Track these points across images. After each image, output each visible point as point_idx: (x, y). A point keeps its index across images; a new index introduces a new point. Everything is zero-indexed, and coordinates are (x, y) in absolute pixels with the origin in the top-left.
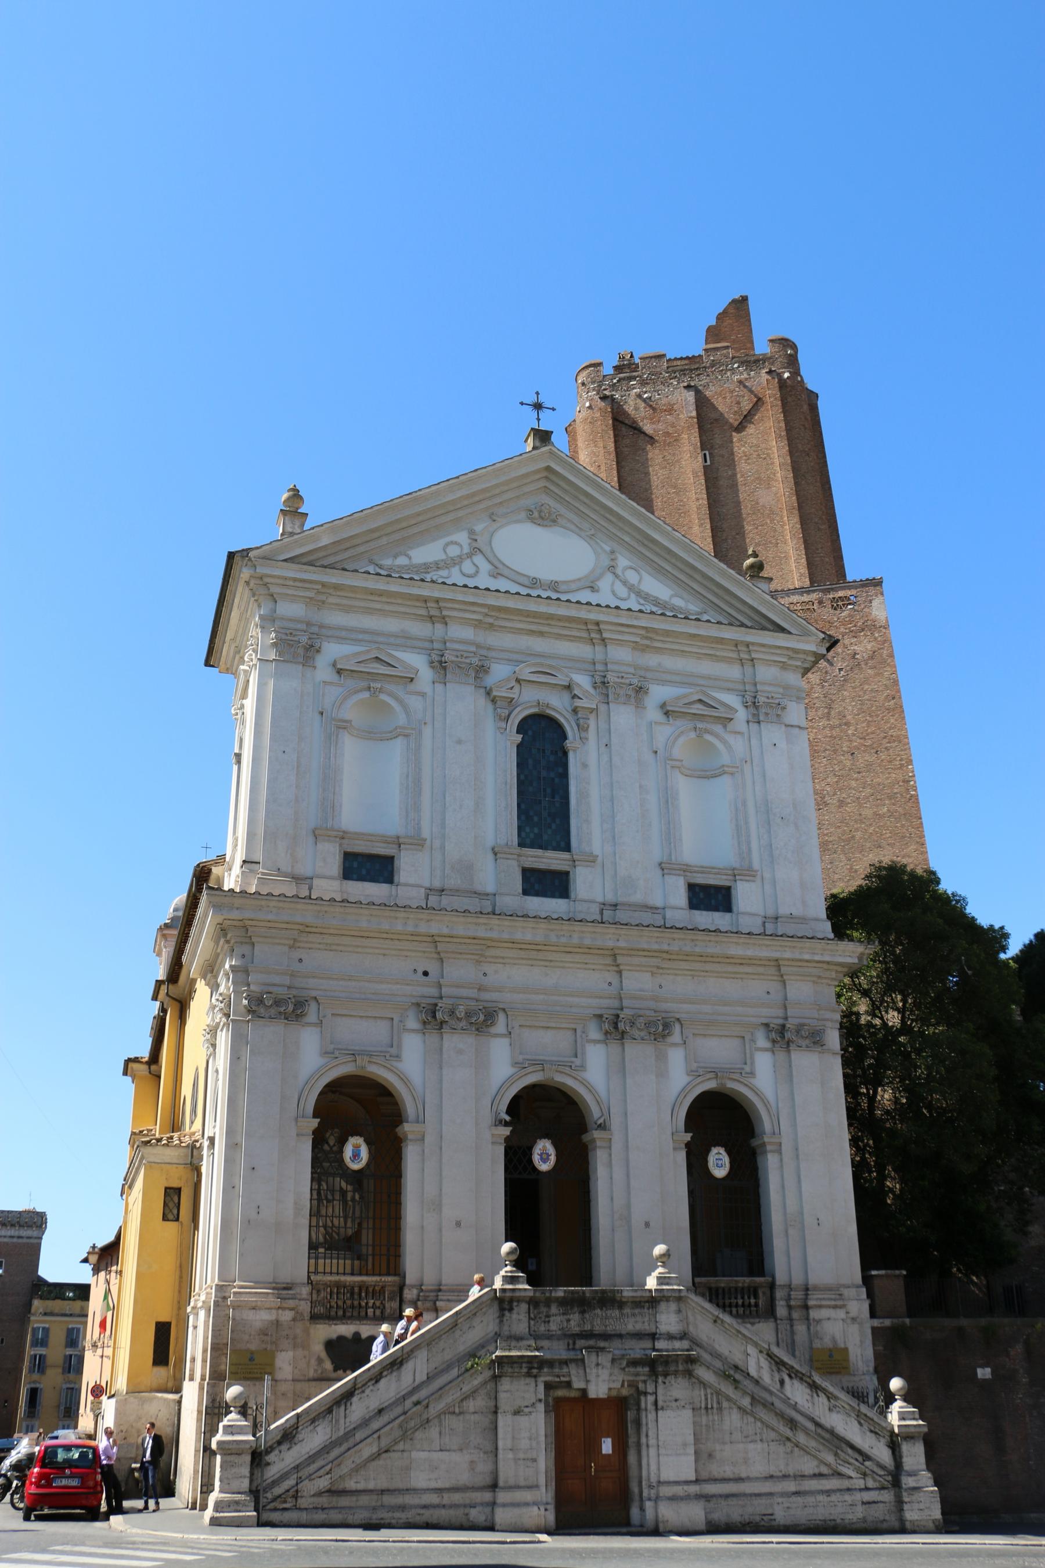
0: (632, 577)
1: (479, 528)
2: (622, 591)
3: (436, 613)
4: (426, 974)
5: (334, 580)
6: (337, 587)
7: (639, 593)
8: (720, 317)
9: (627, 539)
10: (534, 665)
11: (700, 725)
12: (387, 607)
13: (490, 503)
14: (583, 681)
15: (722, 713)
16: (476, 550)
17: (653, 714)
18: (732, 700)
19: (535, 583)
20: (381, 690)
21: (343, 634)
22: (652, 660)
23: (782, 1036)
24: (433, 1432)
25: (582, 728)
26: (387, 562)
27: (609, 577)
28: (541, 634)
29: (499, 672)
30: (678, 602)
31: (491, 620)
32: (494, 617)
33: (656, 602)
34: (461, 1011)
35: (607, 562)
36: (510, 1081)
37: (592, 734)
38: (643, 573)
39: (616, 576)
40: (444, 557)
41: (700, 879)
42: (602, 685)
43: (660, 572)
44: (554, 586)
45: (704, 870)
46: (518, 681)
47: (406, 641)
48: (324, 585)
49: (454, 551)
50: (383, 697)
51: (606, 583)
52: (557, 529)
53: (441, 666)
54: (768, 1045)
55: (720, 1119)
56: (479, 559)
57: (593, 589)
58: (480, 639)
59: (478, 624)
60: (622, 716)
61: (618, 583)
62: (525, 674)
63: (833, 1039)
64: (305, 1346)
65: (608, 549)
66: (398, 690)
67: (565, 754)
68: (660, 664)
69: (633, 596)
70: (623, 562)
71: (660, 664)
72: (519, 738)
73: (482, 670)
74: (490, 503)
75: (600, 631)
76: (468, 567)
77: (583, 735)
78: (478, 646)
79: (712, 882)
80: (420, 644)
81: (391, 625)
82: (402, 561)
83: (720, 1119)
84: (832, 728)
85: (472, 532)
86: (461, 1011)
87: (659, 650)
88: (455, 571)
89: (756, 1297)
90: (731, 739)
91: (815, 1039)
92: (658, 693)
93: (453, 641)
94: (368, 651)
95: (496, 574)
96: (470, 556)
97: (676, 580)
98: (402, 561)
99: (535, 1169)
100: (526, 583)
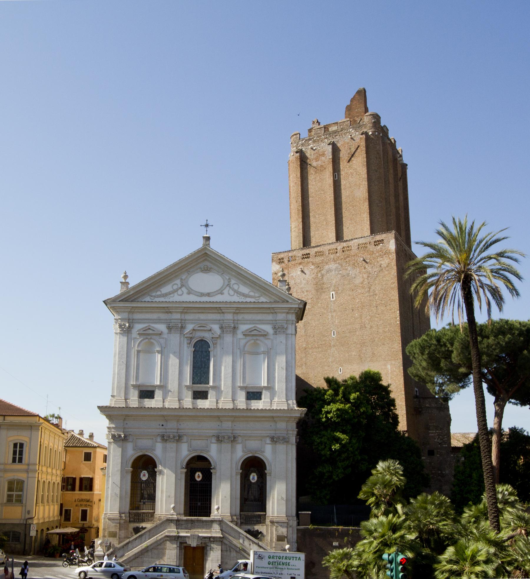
0: (236, 287)
1: (184, 277)
2: (232, 292)
3: (167, 310)
4: (163, 425)
5: (135, 305)
6: (136, 307)
7: (237, 293)
8: (352, 100)
9: (234, 274)
10: (200, 324)
11: (255, 338)
12: (153, 311)
13: (187, 268)
14: (216, 328)
15: (263, 333)
16: (182, 286)
17: (240, 336)
18: (268, 328)
19: (202, 295)
20: (151, 338)
21: (140, 321)
22: (240, 317)
23: (274, 440)
24: (150, 553)
25: (215, 344)
26: (154, 294)
27: (228, 288)
28: (202, 313)
29: (190, 327)
30: (252, 294)
31: (185, 311)
32: (187, 309)
33: (244, 295)
34: (171, 436)
35: (227, 283)
36: (187, 456)
37: (218, 346)
38: (240, 285)
39: (230, 287)
40: (172, 290)
41: (251, 390)
42: (221, 328)
43: (245, 284)
44: (208, 295)
45: (252, 388)
46: (194, 330)
47: (159, 321)
48: (132, 307)
49: (175, 287)
50: (152, 340)
51: (226, 292)
52: (211, 273)
53: (169, 328)
54: (270, 442)
55: (254, 466)
56: (184, 289)
57: (222, 294)
58: (183, 317)
59: (182, 313)
60: (228, 338)
61: (231, 290)
62: (196, 328)
63: (293, 440)
64: (127, 529)
65: (228, 278)
66: (157, 337)
67: (209, 352)
68: (243, 318)
69: (235, 294)
70: (233, 282)
71: (243, 318)
72: (194, 349)
73: (183, 328)
74: (187, 268)
75: (221, 310)
76: (180, 292)
77: (215, 346)
78: (181, 320)
79: (255, 391)
80: (163, 321)
81: (155, 316)
82: (159, 293)
83: (254, 466)
84: (370, 296)
85: (181, 279)
86: (171, 436)
87: (242, 313)
88: (176, 294)
89: (260, 518)
90: (266, 341)
91: (285, 440)
92: (243, 328)
93: (173, 319)
94: (146, 327)
95: (189, 293)
96: (180, 288)
97: (251, 286)
98: (159, 293)
99: (196, 480)
100: (199, 294)
